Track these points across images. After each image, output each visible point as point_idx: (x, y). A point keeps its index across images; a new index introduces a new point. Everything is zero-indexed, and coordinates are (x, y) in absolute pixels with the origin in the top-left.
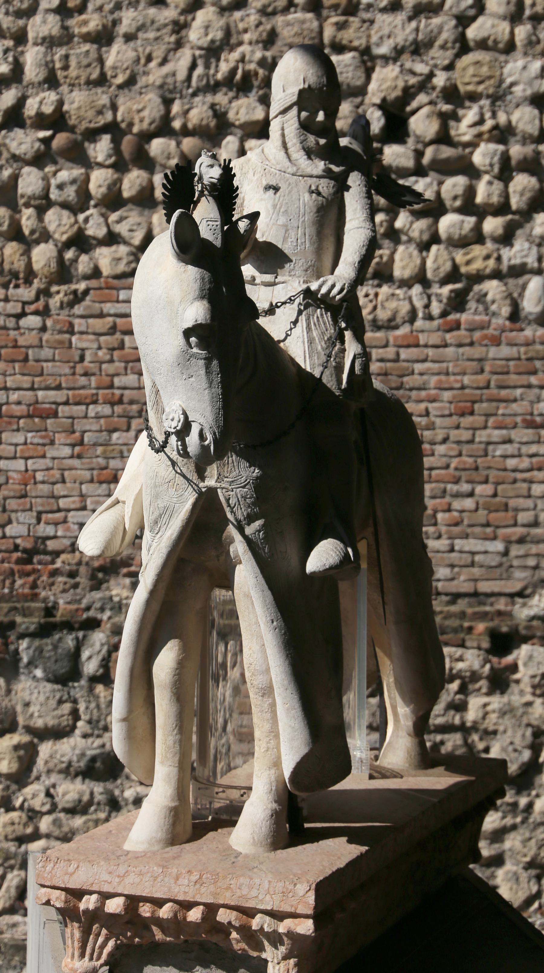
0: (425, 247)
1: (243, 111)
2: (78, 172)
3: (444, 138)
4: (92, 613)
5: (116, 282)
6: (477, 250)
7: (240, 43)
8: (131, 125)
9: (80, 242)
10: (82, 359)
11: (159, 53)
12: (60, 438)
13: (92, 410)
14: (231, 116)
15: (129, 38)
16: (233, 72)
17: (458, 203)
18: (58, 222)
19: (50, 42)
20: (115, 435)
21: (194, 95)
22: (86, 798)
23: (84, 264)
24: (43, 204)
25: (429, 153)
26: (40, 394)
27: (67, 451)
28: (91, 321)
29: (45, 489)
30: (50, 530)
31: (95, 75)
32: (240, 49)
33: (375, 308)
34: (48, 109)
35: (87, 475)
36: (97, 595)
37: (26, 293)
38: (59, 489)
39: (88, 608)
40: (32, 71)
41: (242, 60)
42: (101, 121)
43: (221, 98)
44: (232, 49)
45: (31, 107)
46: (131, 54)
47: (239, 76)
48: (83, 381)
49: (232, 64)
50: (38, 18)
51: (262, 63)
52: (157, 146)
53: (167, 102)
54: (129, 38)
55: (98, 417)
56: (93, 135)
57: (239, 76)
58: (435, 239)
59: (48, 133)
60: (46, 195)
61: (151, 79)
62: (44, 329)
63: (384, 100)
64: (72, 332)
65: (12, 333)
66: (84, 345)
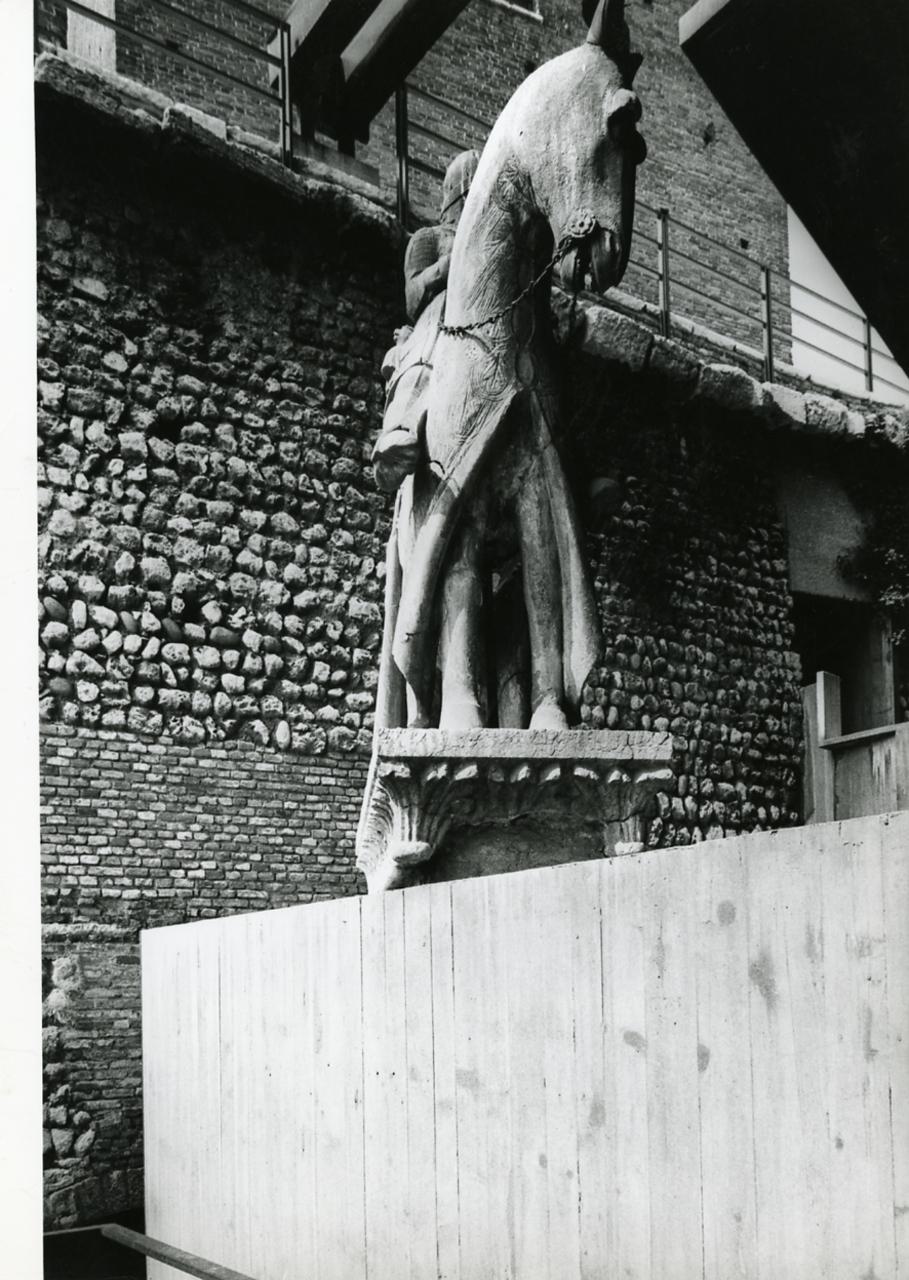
0: (212, 693)
3: (223, 622)
6: (248, 699)
7: (86, 538)
14: (81, 585)
16: (81, 555)
17: (234, 666)
21: (52, 567)
25: (214, 632)
32: (85, 543)
43: (71, 573)
49: (80, 551)
51: (101, 553)
58: (220, 688)
63: (184, 591)
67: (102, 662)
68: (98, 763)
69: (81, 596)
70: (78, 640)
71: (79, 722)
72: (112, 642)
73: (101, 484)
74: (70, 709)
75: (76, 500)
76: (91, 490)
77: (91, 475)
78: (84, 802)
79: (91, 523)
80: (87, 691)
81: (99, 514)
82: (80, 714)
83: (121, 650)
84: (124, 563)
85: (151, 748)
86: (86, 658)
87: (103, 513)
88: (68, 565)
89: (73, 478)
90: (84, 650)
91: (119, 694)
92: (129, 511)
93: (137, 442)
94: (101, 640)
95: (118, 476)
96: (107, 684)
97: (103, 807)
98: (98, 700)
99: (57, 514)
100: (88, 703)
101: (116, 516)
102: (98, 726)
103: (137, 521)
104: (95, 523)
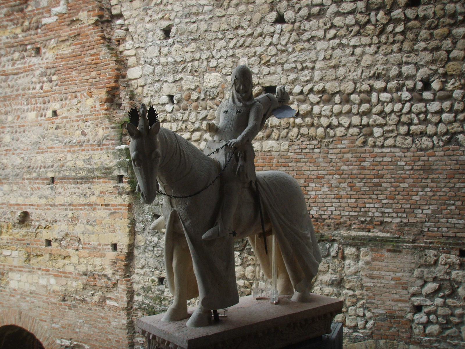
0: (437, 124)
1: (378, 85)
2: (330, 107)
3: (442, 89)
4: (334, 238)
5: (341, 138)
6: (455, 125)
7: (377, 64)
8: (345, 91)
9: (330, 126)
10: (331, 161)
11: (352, 70)
12: (325, 185)
13: (335, 176)
14: (375, 86)
15: (344, 65)
16: (374, 73)
17: (448, 110)
18: (324, 121)
19: (321, 69)
20: (341, 184)
21: (363, 81)
22: (331, 292)
23: (332, 133)
24: (320, 116)
25: (438, 94)
26: (320, 172)
27: (327, 189)
28: (334, 150)
29: (321, 200)
30: (323, 213)
31: (334, 77)
32: (377, 66)
33: (421, 144)
34: (321, 88)
35: (333, 196)
36: (336, 232)
37: (315, 142)
38: (325, 200)
39: (333, 236)
40: (316, 79)
41: (377, 69)
42: (336, 90)
43: (371, 82)
44: (375, 66)
45: (316, 88)
46: (344, 70)
47: (376, 75)
48: (332, 168)
50: (318, 63)
51: (383, 70)
52: (353, 97)
53: (355, 84)
54: (344, 65)
55: (336, 179)
56: (333, 95)
57: (376, 75)
58: (440, 121)
59: (320, 95)
60: (320, 114)
61: (349, 78)
62: (320, 152)
63: (422, 78)
64: (328, 153)
65: (312, 155)
66: (332, 157)
67: (384, 118)
68: (382, 163)
69: (375, 90)
70: (375, 110)
71: (375, 146)
72: (388, 109)
73: (383, 39)
74: (370, 140)
75: (373, 49)
76: (379, 42)
77: (378, 36)
78: (376, 181)
79: (379, 56)
80: (377, 132)
81: (382, 53)
82: (375, 142)
83: (392, 111)
84: (394, 71)
85: (406, 154)
86: (377, 117)
87: (384, 51)
88: (370, 78)
89: (372, 39)
90: (376, 114)
91: (392, 131)
92: (395, 47)
93: (399, 14)
94: (384, 108)
95: (391, 32)
96: (386, 128)
97: (384, 182)
98: (383, 136)
99: (365, 57)
100: (378, 137)
101: (390, 51)
102: (383, 146)
103: (400, 50)
104: (381, 56)
